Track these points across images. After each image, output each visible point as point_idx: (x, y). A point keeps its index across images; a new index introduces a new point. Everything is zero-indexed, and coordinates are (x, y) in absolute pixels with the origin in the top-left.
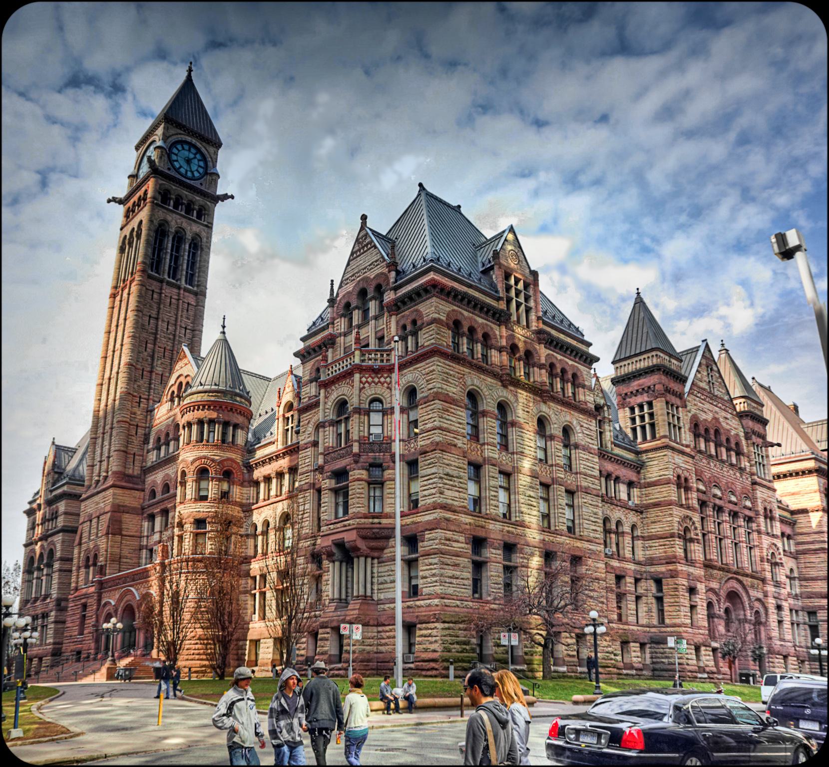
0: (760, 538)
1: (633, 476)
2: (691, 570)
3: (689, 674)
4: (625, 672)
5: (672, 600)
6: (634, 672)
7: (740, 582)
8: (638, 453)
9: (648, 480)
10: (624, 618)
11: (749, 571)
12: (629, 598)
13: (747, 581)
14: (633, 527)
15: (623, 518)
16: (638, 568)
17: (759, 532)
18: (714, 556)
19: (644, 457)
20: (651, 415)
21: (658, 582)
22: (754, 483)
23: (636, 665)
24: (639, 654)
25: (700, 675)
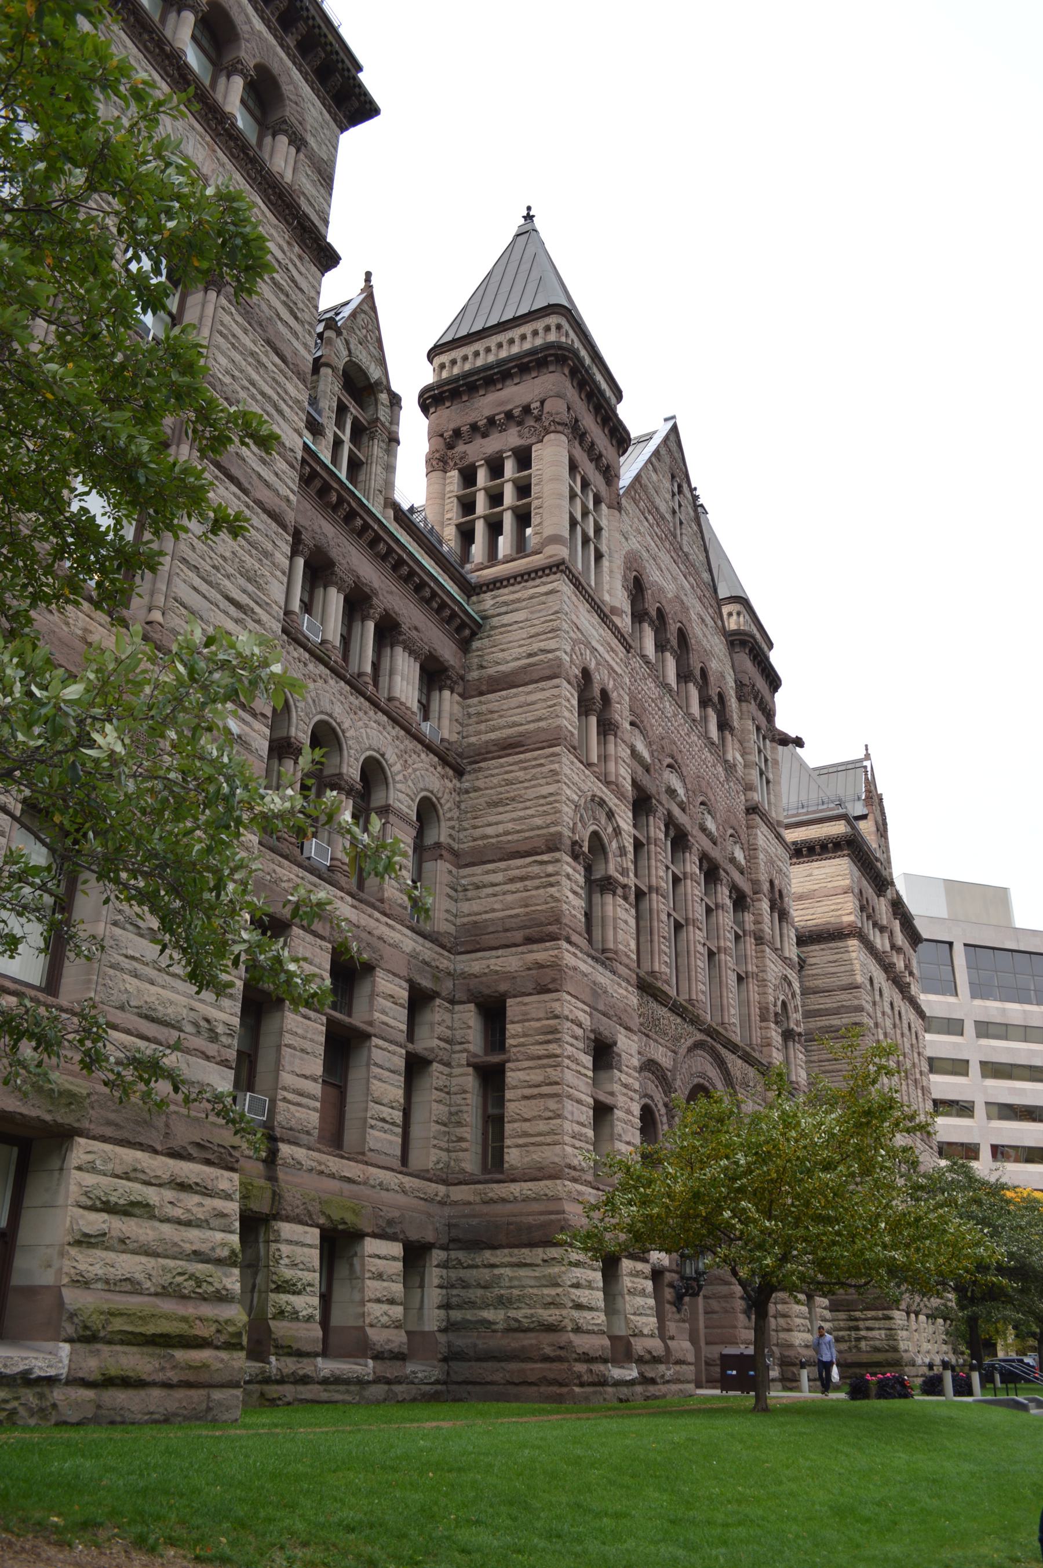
0: (761, 956)
1: (447, 651)
2: (603, 977)
3: (580, 1368)
4: (326, 1367)
5: (536, 1076)
6: (368, 1368)
7: (721, 1063)
8: (471, 590)
9: (491, 671)
10: (350, 1136)
11: (737, 1039)
12: (377, 1055)
13: (736, 1065)
14: (427, 810)
15: (391, 756)
16: (427, 951)
17: (759, 940)
18: (662, 965)
19: (488, 601)
20: (524, 490)
21: (493, 1013)
22: (752, 810)
23: (376, 1336)
24: (397, 1288)
25: (616, 1373)
